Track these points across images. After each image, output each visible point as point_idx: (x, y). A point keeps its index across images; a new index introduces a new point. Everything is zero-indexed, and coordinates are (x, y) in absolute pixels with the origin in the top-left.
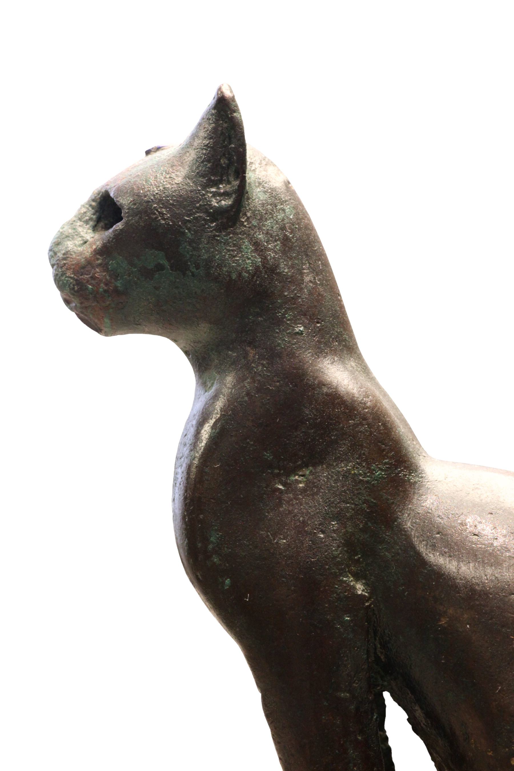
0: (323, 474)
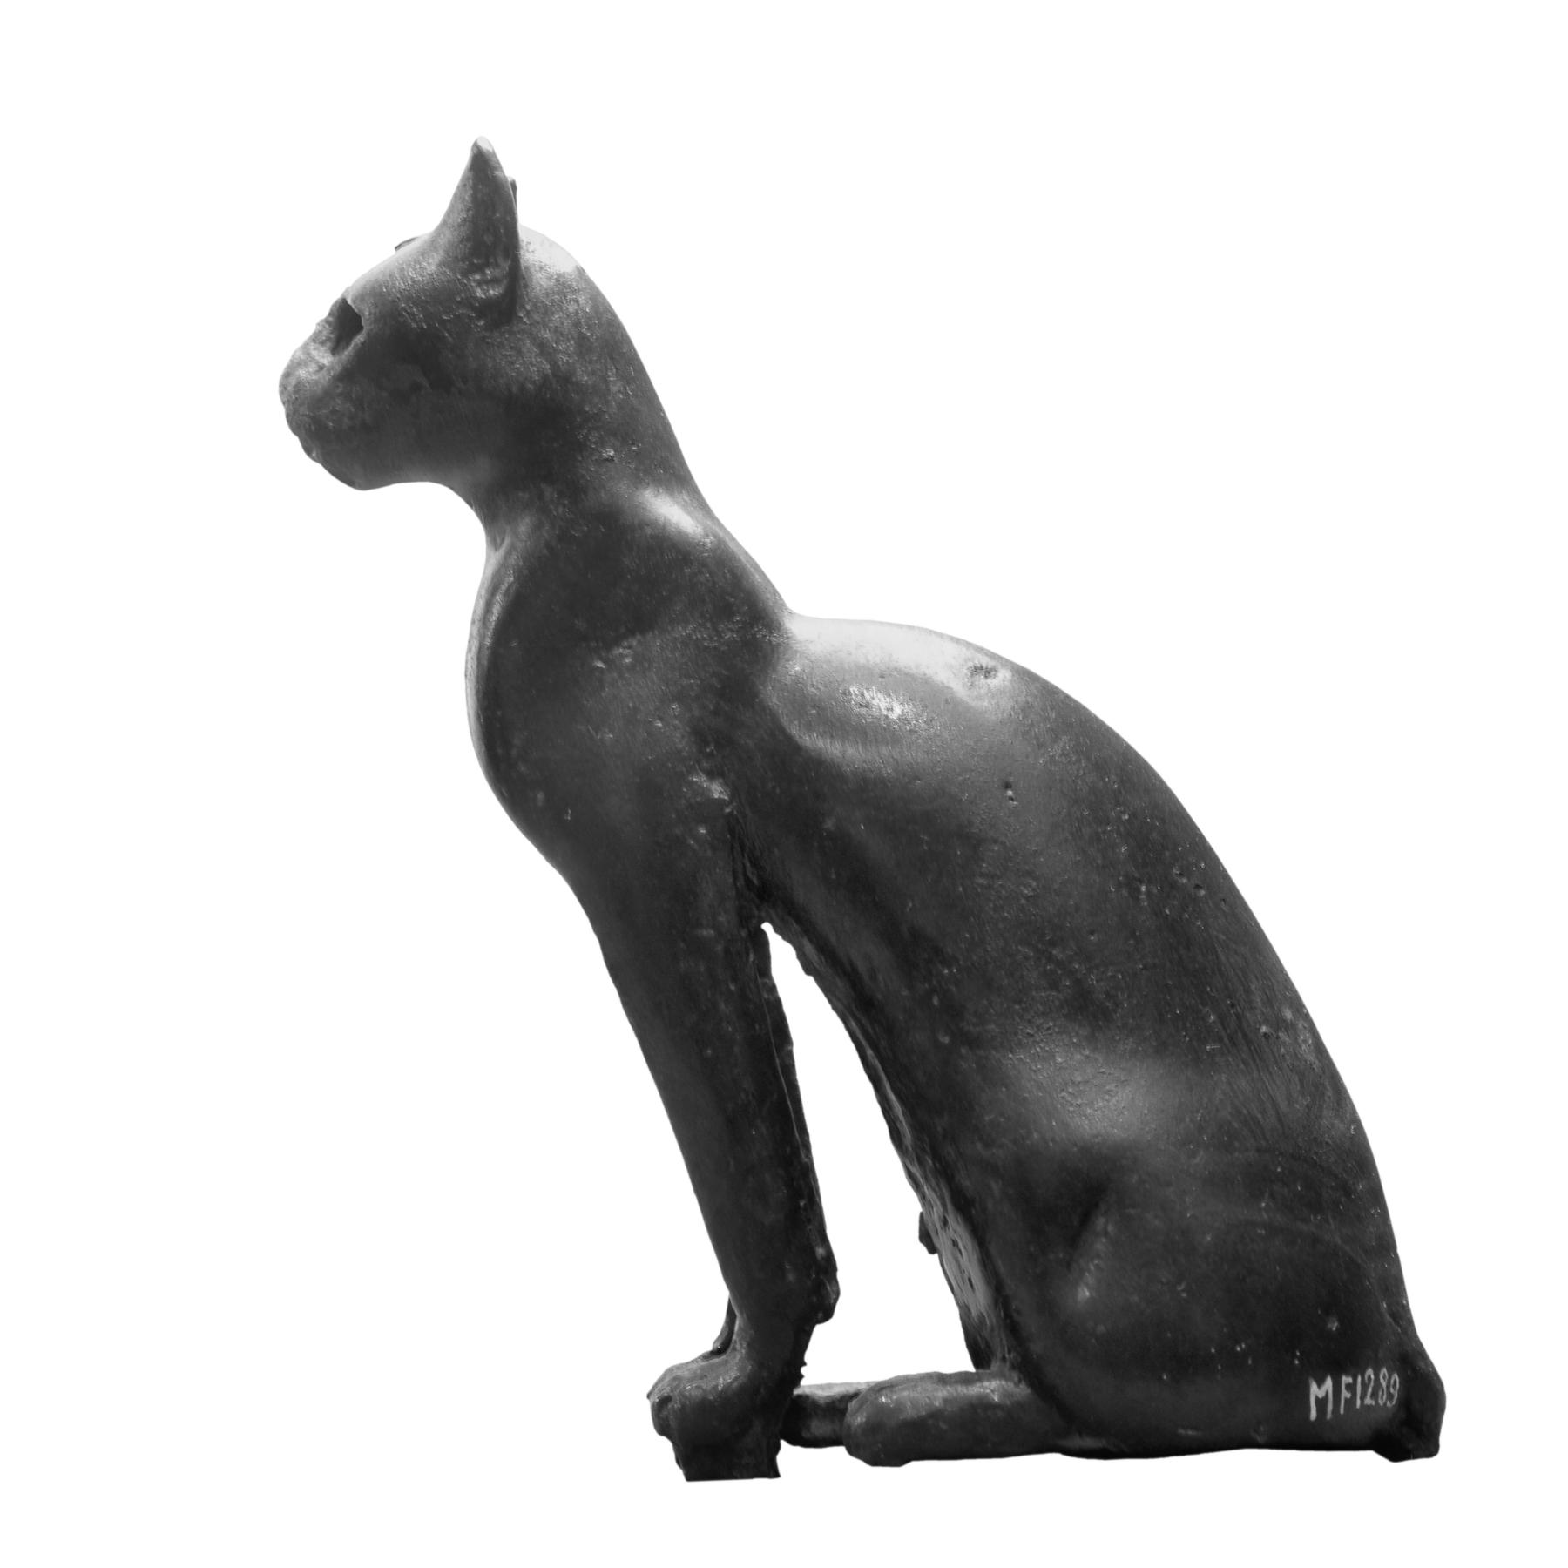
0: (655, 642)
